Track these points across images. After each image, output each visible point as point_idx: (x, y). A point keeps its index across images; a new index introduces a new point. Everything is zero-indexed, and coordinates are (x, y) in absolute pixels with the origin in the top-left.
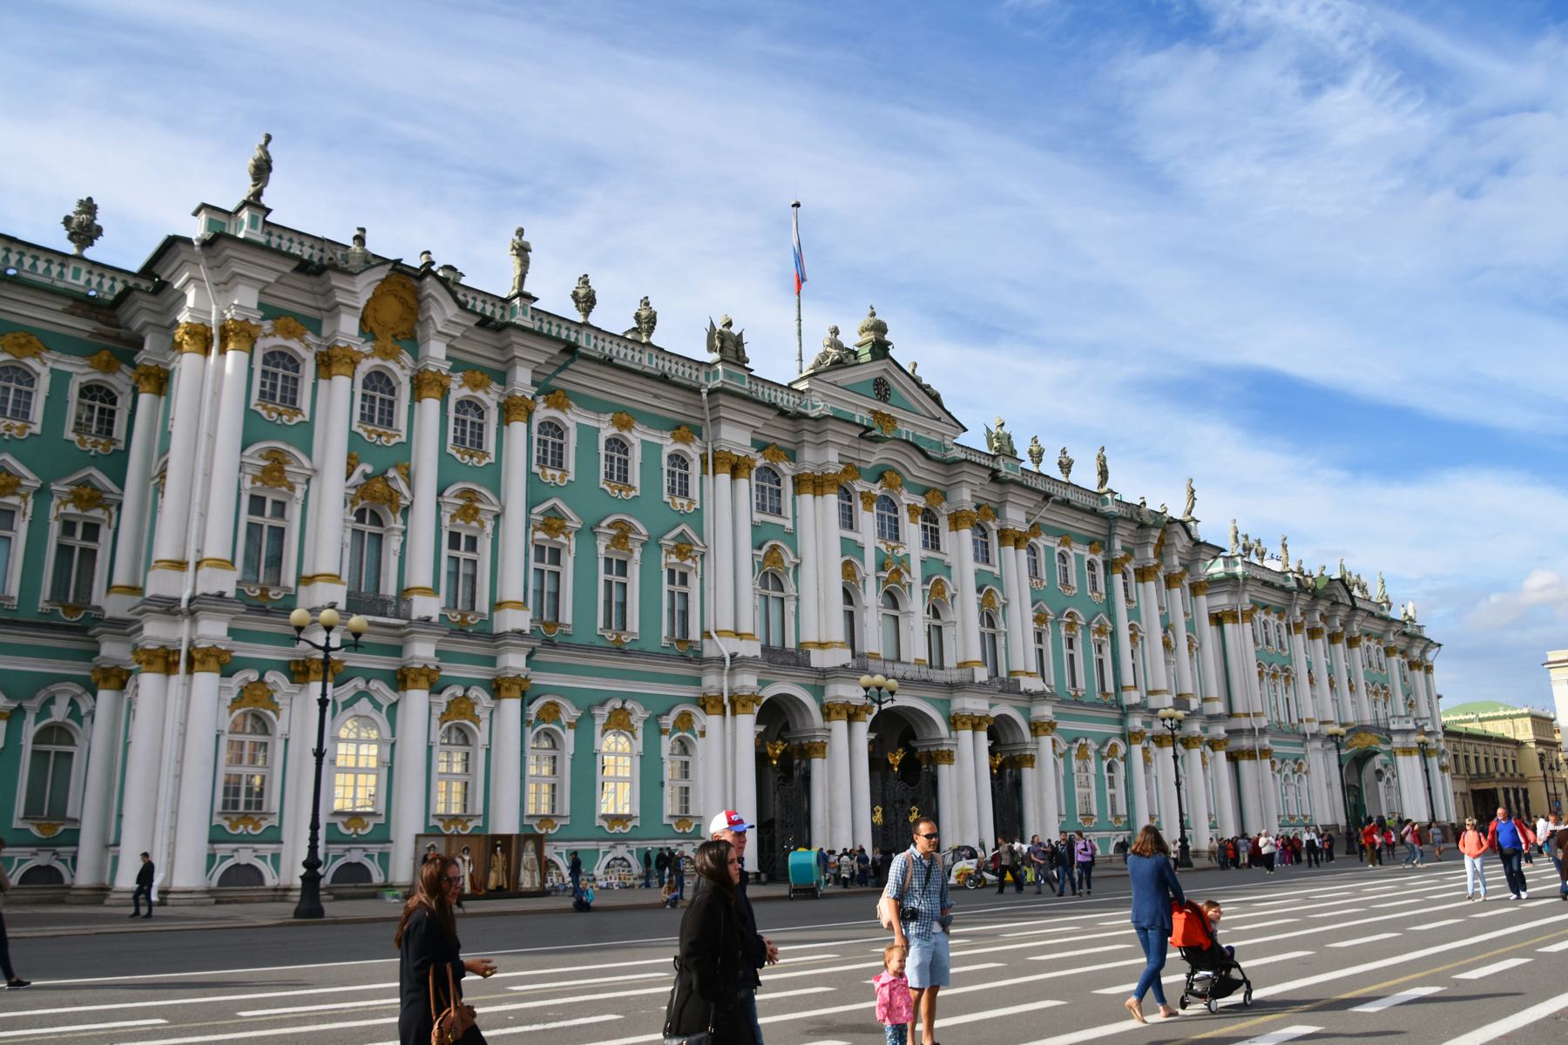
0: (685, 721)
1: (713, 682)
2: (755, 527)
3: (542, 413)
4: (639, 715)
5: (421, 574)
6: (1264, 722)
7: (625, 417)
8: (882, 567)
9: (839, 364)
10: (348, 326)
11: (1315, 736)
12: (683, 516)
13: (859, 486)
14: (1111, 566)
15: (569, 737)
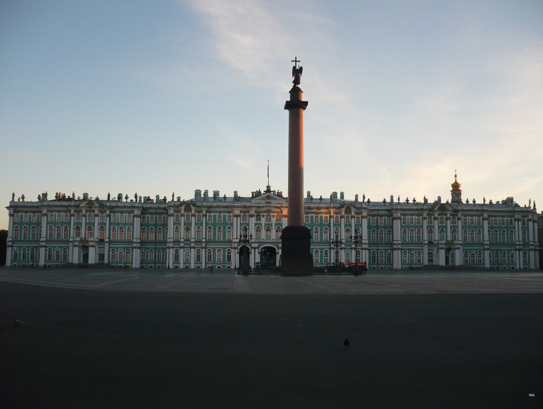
0: (229, 250)
1: (233, 246)
2: (241, 223)
3: (208, 214)
4: (222, 250)
5: (193, 236)
6: (400, 242)
7: (220, 212)
8: (265, 226)
9: (258, 196)
10: (183, 211)
11: (424, 244)
12: (229, 224)
13: (261, 214)
14: (330, 217)
15: (212, 253)
